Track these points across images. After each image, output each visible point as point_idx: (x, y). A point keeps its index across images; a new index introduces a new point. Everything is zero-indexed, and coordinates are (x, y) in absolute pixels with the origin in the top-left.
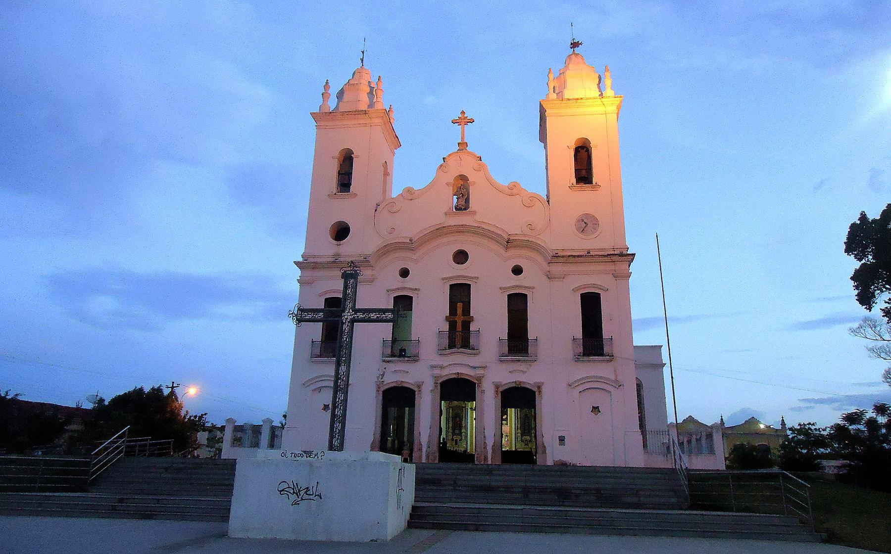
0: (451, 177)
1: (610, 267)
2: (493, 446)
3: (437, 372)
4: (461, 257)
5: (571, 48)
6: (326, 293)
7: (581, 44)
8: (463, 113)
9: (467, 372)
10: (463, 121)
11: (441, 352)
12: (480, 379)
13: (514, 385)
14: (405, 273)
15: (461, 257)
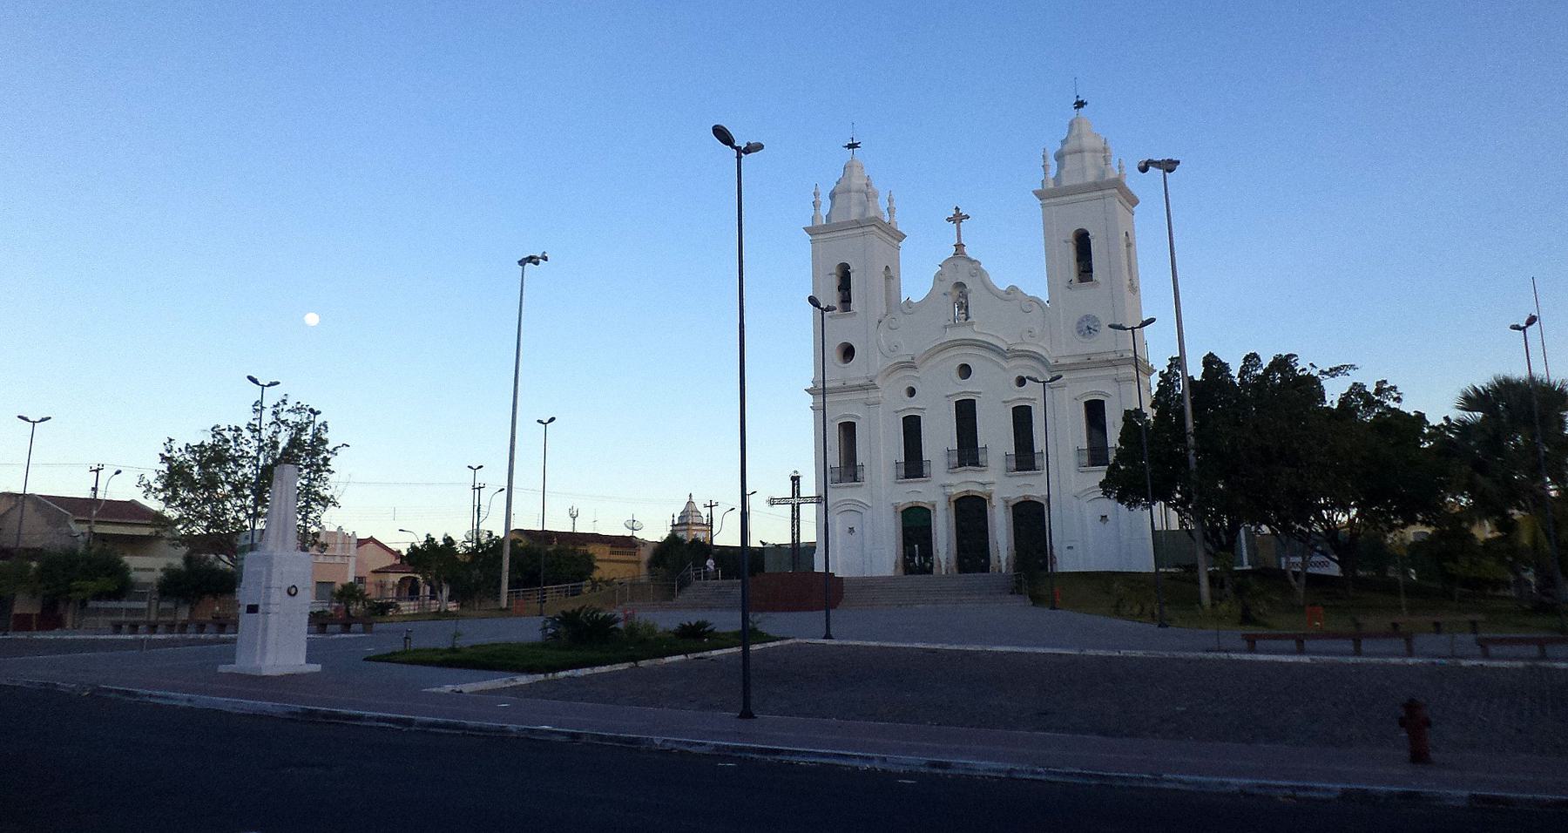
0: (948, 286)
1: (1113, 371)
2: (1007, 559)
3: (948, 490)
4: (965, 371)
5: (1075, 108)
6: (841, 417)
7: (1086, 103)
8: (957, 209)
9: (976, 489)
10: (958, 218)
11: (952, 469)
12: (990, 497)
13: (1021, 500)
14: (912, 392)
15: (965, 371)
